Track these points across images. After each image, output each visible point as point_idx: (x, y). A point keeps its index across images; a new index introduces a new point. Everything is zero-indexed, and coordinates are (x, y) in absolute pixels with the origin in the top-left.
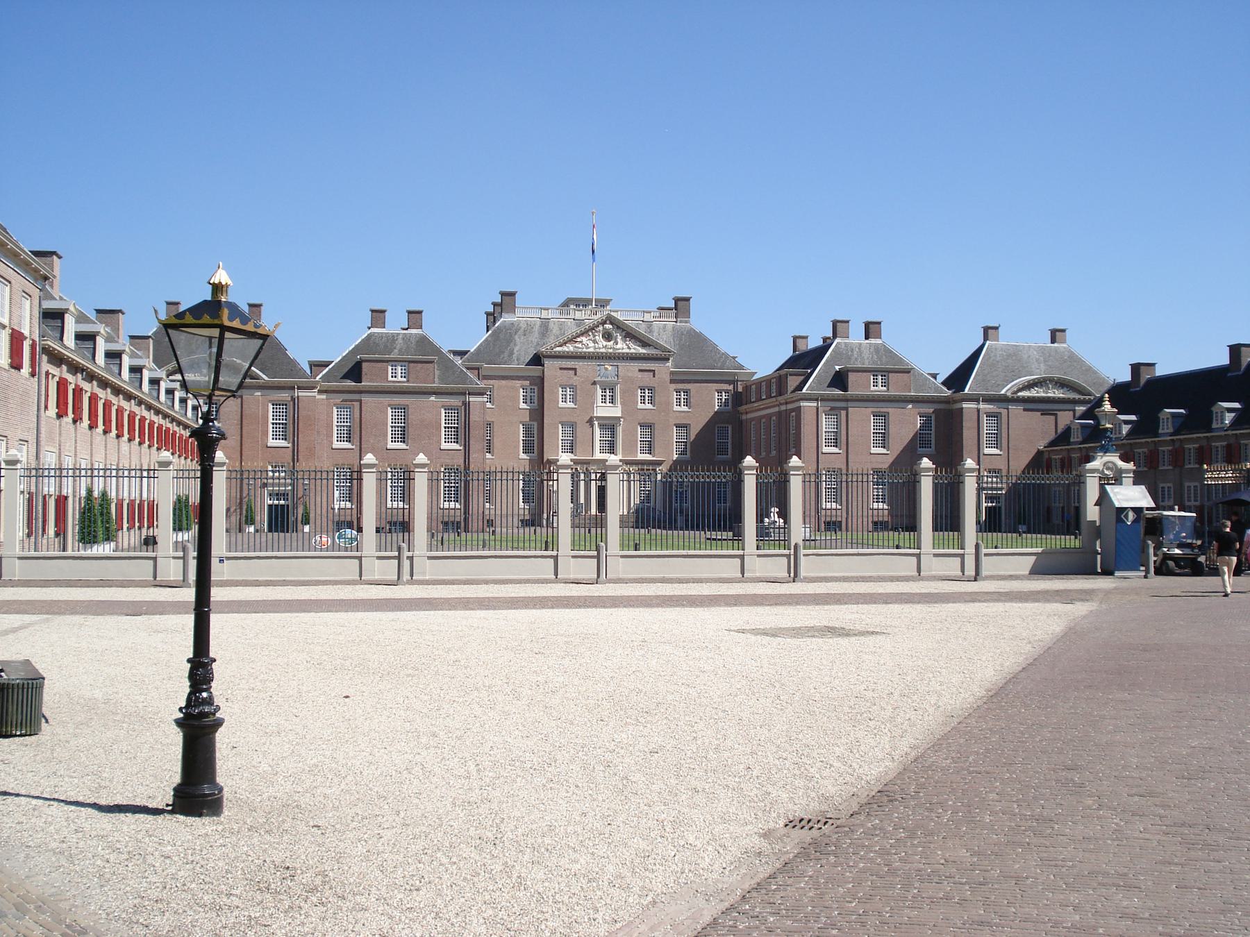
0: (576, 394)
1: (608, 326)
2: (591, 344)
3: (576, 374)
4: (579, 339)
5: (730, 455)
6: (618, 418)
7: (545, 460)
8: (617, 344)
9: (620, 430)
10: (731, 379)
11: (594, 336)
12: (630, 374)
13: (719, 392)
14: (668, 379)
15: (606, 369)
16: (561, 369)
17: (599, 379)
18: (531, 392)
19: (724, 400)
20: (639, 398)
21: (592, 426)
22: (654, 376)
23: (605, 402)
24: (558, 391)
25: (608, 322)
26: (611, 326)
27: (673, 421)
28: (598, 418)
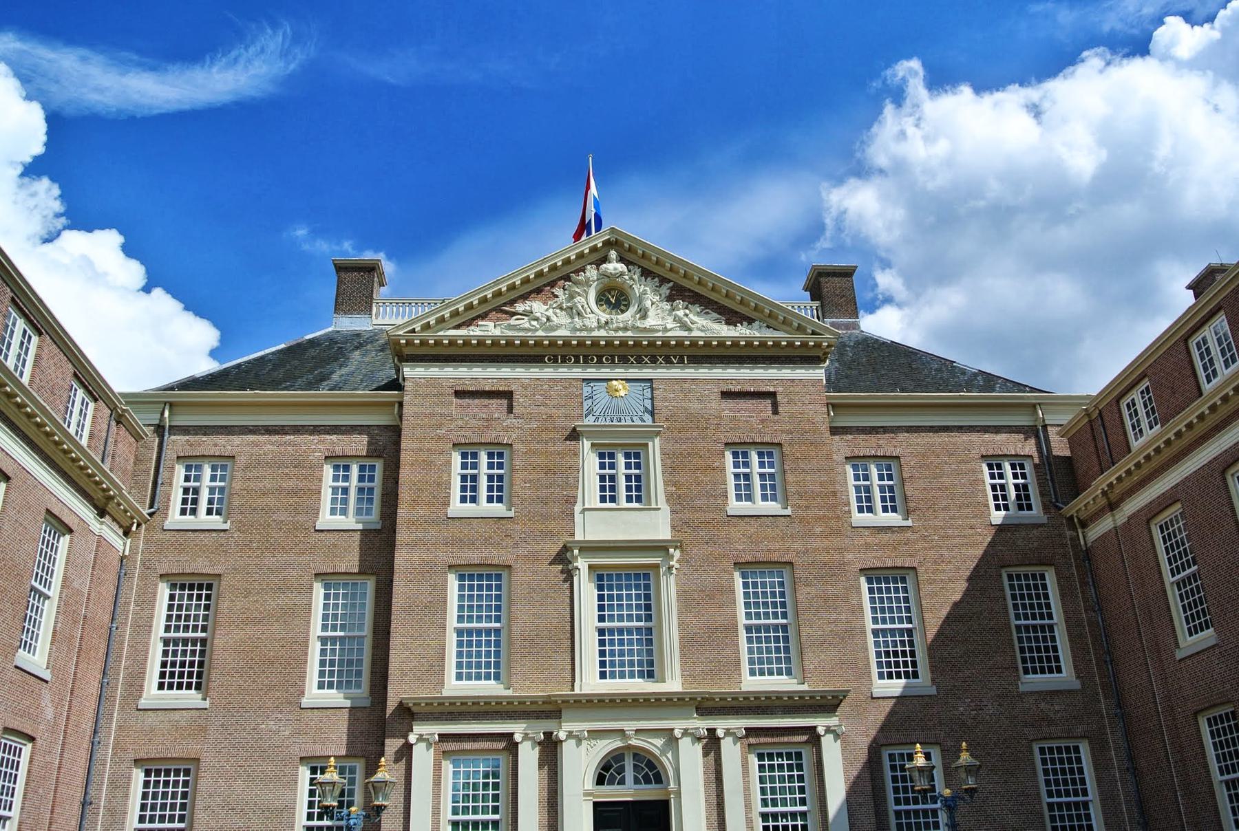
0: (512, 470)
1: (614, 266)
2: (561, 319)
3: (510, 410)
4: (520, 307)
5: (1067, 676)
6: (660, 548)
7: (391, 705)
8: (644, 317)
9: (669, 589)
10: (1023, 420)
11: (571, 297)
12: (695, 407)
13: (994, 463)
14: (820, 417)
15: (612, 392)
16: (459, 394)
17: (590, 421)
18: (361, 479)
19: (1012, 494)
20: (731, 482)
21: (569, 576)
22: (775, 412)
23: (613, 499)
24: (449, 462)
25: (613, 254)
26: (621, 267)
27: (855, 560)
28: (590, 548)
